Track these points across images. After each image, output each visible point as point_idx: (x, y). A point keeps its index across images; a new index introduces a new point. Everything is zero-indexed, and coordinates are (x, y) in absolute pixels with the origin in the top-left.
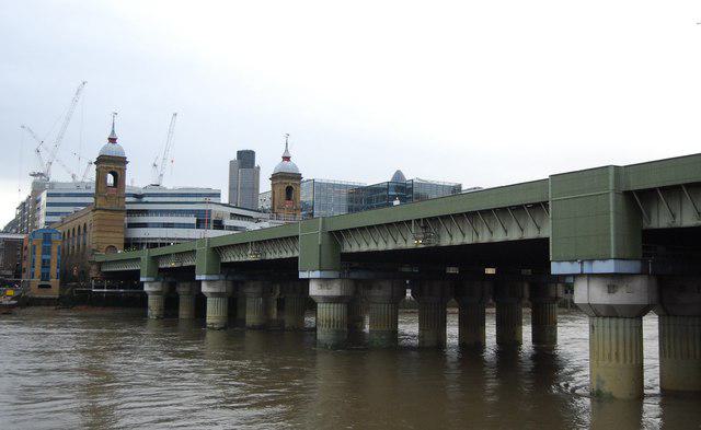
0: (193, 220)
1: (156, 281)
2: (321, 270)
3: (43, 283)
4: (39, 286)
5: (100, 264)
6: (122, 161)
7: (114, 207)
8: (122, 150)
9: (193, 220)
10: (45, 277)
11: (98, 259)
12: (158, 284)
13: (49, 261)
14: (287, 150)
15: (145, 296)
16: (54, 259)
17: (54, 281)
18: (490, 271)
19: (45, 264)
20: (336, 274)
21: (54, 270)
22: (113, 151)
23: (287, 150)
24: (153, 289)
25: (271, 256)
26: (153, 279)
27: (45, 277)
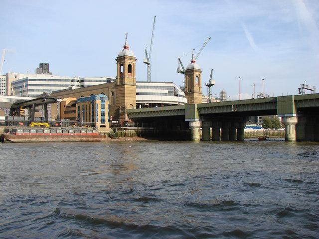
0: (166, 91)
3: (102, 124)
4: (101, 126)
9: (166, 91)
10: (103, 121)
17: (107, 124)
27: (103, 121)
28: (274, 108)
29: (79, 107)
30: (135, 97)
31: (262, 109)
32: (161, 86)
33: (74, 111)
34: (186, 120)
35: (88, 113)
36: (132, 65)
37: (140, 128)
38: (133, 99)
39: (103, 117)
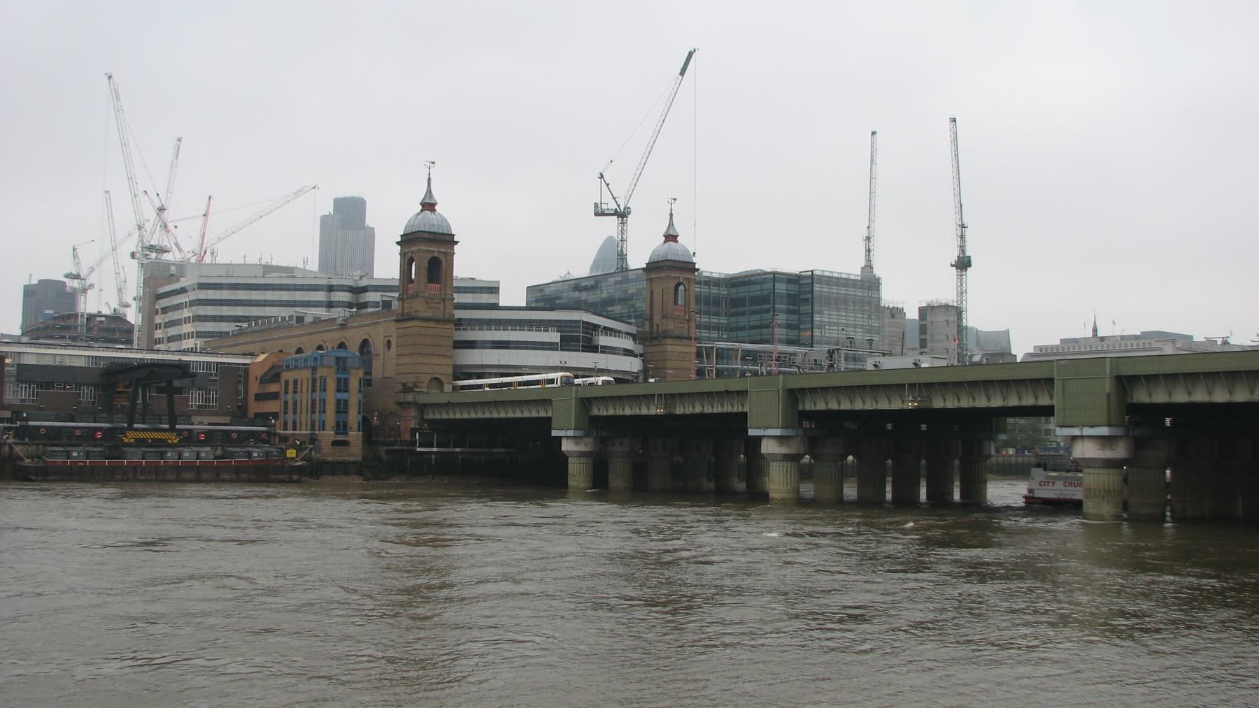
0: (554, 337)
1: (587, 435)
2: (1109, 425)
3: (340, 438)
4: (335, 443)
5: (423, 408)
6: (447, 240)
7: (439, 315)
8: (449, 227)
9: (554, 337)
11: (423, 399)
12: (590, 440)
13: (346, 402)
14: (671, 225)
15: (563, 459)
16: (354, 397)
17: (355, 435)
18: (924, 427)
19: (342, 407)
20: (1117, 431)
21: (354, 417)
22: (429, 222)
23: (671, 225)
24: (582, 448)
25: (938, 404)
26: (580, 433)
27: (341, 427)
28: (740, 410)
29: (287, 382)
30: (451, 357)
31: (725, 410)
32: (540, 321)
33: (275, 396)
34: (554, 433)
35: (304, 402)
36: (442, 258)
37: (458, 450)
38: (444, 361)
39: (342, 415)
